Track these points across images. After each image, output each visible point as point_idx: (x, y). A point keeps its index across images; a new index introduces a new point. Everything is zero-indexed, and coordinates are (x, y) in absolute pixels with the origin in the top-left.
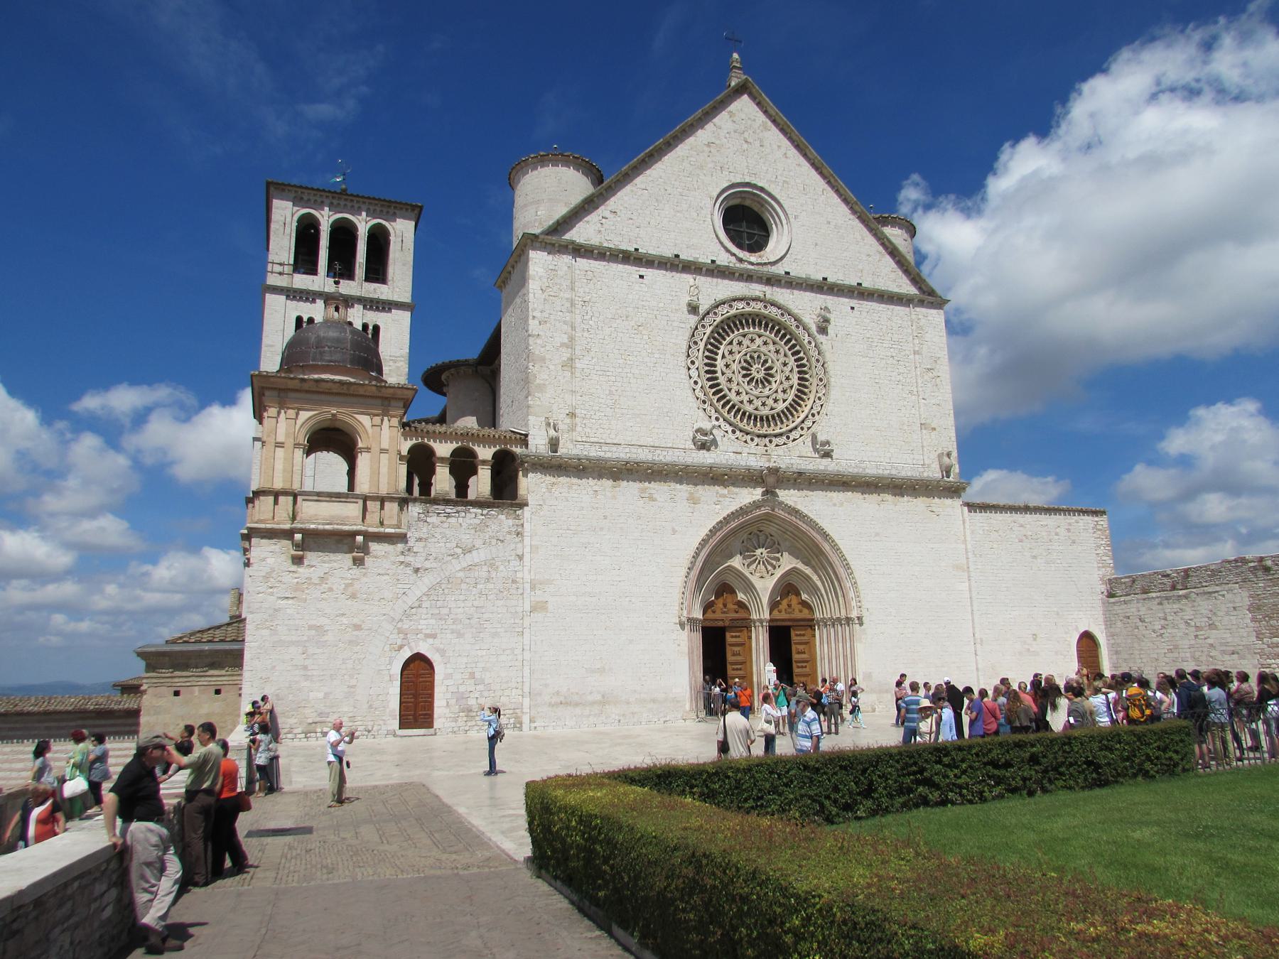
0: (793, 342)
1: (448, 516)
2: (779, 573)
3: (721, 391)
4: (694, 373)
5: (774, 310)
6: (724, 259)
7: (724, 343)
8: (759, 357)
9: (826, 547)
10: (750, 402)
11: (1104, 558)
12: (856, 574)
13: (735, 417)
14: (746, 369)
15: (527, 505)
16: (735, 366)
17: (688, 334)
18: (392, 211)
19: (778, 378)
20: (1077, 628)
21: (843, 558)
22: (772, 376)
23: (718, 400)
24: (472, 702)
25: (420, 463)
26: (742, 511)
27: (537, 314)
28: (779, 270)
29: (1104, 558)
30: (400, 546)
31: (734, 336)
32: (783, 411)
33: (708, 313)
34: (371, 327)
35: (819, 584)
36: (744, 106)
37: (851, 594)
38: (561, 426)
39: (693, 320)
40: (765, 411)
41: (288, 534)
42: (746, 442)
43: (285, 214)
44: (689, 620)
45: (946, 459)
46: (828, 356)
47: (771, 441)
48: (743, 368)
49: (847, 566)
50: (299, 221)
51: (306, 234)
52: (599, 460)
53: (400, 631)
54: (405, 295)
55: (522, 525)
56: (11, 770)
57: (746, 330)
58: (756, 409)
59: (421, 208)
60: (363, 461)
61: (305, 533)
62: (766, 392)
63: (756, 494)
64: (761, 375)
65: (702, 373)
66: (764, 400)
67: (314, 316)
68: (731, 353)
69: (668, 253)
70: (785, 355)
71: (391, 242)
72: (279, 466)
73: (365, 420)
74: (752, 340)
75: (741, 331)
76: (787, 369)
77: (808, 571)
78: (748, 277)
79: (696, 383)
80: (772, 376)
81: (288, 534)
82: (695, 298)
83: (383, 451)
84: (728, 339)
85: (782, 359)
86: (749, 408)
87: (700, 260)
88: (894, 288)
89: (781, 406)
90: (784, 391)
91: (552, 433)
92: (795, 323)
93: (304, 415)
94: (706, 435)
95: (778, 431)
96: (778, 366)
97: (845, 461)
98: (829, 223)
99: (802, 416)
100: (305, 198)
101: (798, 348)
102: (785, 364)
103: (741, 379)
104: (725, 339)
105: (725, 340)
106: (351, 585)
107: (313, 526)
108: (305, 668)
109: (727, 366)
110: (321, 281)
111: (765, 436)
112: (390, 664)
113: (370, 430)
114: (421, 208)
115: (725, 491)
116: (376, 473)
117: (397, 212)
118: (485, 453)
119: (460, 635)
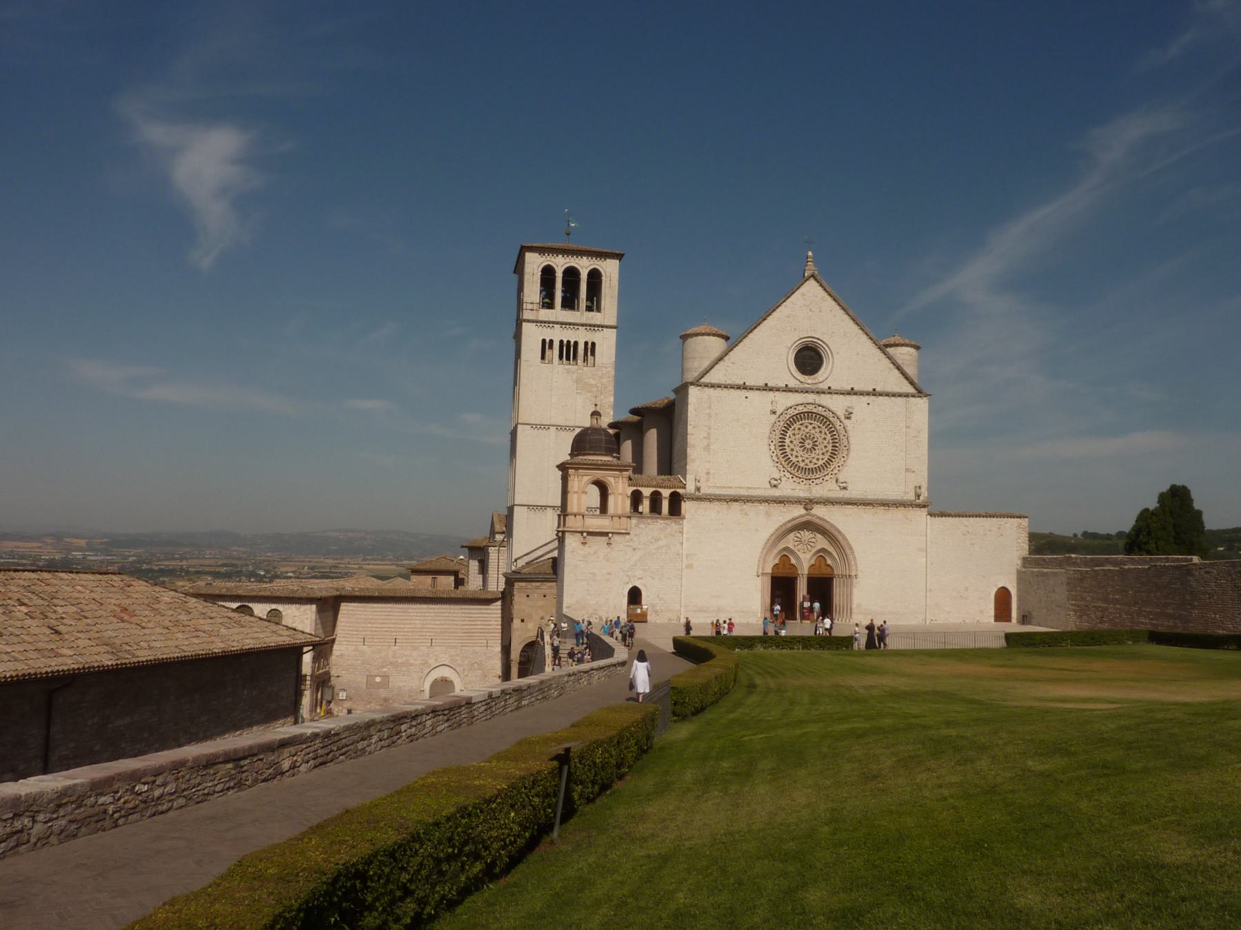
0: (831, 426)
1: (649, 524)
2: (814, 550)
3: (787, 455)
4: (773, 448)
5: (820, 408)
6: (793, 383)
7: (790, 429)
8: (810, 436)
9: (840, 538)
10: (803, 461)
11: (1022, 545)
12: (856, 553)
13: (794, 469)
14: (802, 443)
15: (685, 518)
17: (771, 426)
19: (820, 447)
20: (996, 585)
21: (849, 545)
22: (817, 446)
23: (785, 461)
24: (658, 608)
25: (636, 498)
26: (794, 519)
27: (692, 423)
28: (824, 386)
29: (1022, 545)
30: (628, 537)
31: (797, 426)
32: (821, 465)
33: (782, 414)
34: (590, 344)
35: (837, 557)
36: (811, 288)
37: (853, 563)
38: (702, 480)
39: (774, 417)
40: (811, 466)
42: (799, 483)
43: (534, 263)
44: (763, 574)
45: (918, 489)
46: (850, 433)
47: (813, 482)
48: (800, 442)
49: (851, 549)
50: (542, 271)
52: (720, 495)
53: (627, 576)
54: (613, 322)
55: (683, 528)
56: (435, 624)
57: (803, 421)
58: (807, 465)
59: (623, 255)
60: (611, 499)
62: (813, 455)
63: (803, 512)
65: (777, 447)
66: (810, 459)
67: (552, 338)
68: (794, 434)
69: (762, 384)
70: (825, 434)
71: (603, 282)
72: (575, 501)
73: (611, 479)
74: (807, 427)
75: (801, 422)
76: (826, 442)
77: (830, 549)
79: (773, 452)
80: (817, 446)
81: (582, 533)
82: (774, 408)
83: (620, 494)
84: (793, 427)
85: (823, 437)
86: (802, 465)
87: (780, 385)
88: (897, 390)
89: (821, 462)
90: (823, 454)
91: (698, 484)
92: (831, 415)
93: (586, 478)
94: (776, 480)
95: (818, 476)
96: (820, 440)
97: (854, 492)
98: (858, 354)
99: (832, 467)
101: (833, 429)
102: (825, 439)
103: (798, 449)
104: (791, 427)
105: (791, 427)
106: (607, 555)
107: (591, 530)
108: (588, 590)
109: (791, 442)
110: (558, 313)
111: (810, 479)
112: (623, 589)
113: (613, 484)
114: (623, 255)
115: (785, 510)
116: (616, 504)
118: (666, 493)
119: (654, 579)
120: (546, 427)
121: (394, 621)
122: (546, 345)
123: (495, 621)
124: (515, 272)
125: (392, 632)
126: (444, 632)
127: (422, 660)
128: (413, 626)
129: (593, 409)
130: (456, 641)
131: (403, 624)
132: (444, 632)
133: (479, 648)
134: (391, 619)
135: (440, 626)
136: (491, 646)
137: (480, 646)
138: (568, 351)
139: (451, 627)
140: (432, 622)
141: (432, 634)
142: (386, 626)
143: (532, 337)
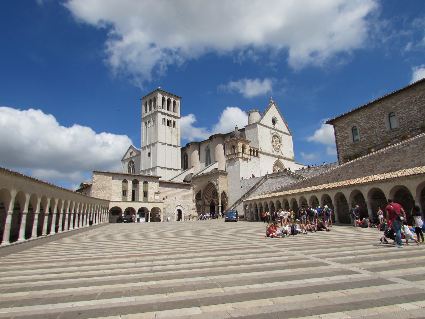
6: (273, 127)
9: (283, 167)
16: (274, 142)
18: (177, 98)
28: (277, 129)
41: (242, 158)
43: (160, 96)
51: (163, 100)
53: (251, 171)
59: (182, 98)
61: (245, 158)
64: (276, 143)
69: (268, 126)
78: (275, 130)
89: (278, 147)
91: (261, 148)
93: (242, 144)
97: (285, 156)
100: (163, 93)
117: (178, 98)
118: (256, 150)
120: (164, 144)
121: (166, 191)
122: (164, 120)
123: (191, 192)
124: (141, 99)
125: (165, 194)
126: (179, 195)
127: (174, 204)
128: (170, 192)
129: (236, 126)
130: (182, 198)
131: (168, 192)
132: (179, 195)
133: (187, 200)
134: (164, 190)
135: (177, 193)
136: (190, 200)
137: (188, 200)
138: (169, 121)
139: (180, 193)
140: (175, 191)
141: (176, 195)
142: (164, 192)
143: (160, 117)
